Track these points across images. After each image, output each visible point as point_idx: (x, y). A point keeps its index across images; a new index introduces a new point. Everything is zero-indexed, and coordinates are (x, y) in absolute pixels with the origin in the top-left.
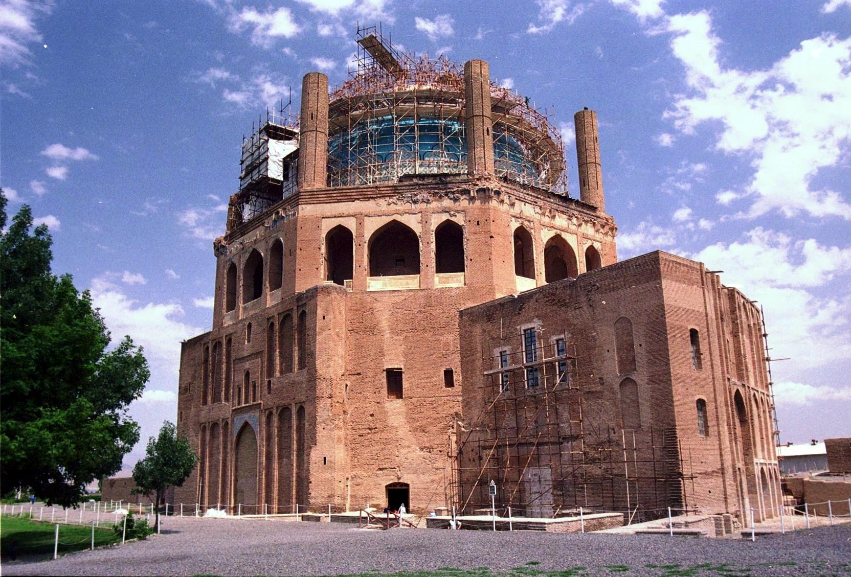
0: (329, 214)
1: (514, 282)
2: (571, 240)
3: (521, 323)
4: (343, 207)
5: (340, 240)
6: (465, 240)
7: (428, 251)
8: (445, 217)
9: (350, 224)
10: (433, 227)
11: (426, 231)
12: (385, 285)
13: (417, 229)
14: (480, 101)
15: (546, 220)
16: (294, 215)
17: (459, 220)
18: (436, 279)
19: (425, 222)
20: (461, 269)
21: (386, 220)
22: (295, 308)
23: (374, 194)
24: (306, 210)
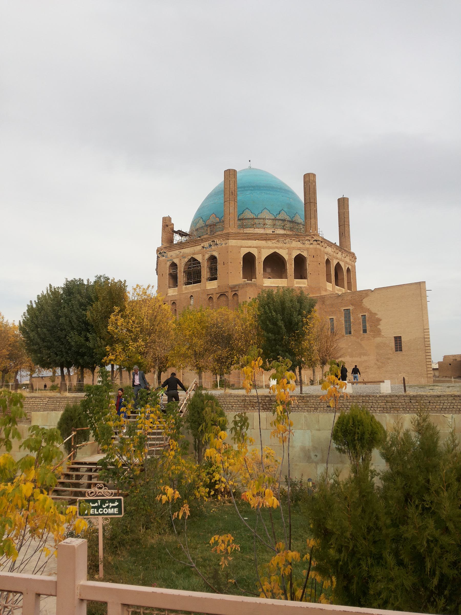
0: (244, 245)
1: (326, 285)
2: (342, 264)
3: (342, 307)
4: (250, 243)
5: (249, 260)
6: (307, 264)
7: (290, 267)
8: (298, 252)
9: (254, 252)
10: (294, 257)
11: (290, 259)
12: (271, 283)
13: (286, 257)
14: (313, 195)
15: (335, 254)
16: (226, 244)
17: (305, 254)
18: (295, 282)
19: (290, 254)
20: (305, 278)
21: (272, 251)
22: (230, 291)
23: (265, 237)
24: (232, 242)
